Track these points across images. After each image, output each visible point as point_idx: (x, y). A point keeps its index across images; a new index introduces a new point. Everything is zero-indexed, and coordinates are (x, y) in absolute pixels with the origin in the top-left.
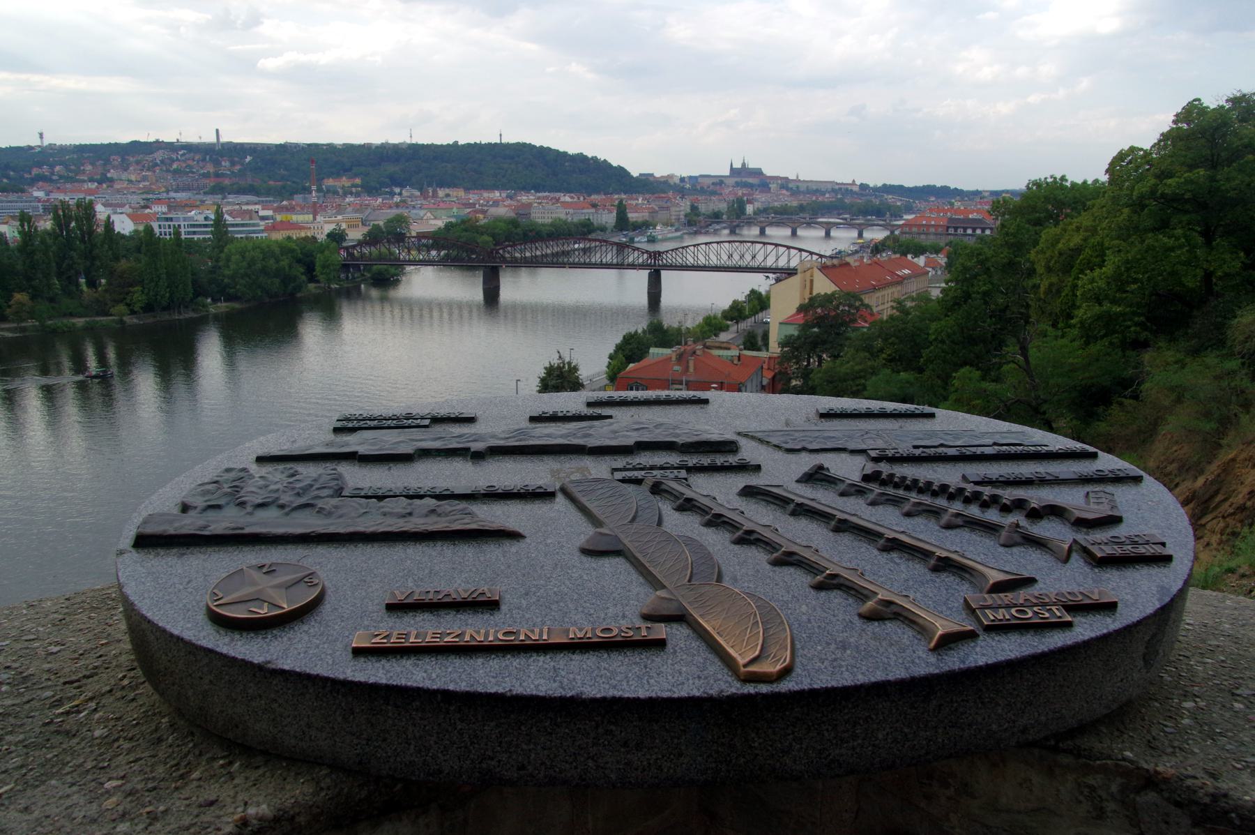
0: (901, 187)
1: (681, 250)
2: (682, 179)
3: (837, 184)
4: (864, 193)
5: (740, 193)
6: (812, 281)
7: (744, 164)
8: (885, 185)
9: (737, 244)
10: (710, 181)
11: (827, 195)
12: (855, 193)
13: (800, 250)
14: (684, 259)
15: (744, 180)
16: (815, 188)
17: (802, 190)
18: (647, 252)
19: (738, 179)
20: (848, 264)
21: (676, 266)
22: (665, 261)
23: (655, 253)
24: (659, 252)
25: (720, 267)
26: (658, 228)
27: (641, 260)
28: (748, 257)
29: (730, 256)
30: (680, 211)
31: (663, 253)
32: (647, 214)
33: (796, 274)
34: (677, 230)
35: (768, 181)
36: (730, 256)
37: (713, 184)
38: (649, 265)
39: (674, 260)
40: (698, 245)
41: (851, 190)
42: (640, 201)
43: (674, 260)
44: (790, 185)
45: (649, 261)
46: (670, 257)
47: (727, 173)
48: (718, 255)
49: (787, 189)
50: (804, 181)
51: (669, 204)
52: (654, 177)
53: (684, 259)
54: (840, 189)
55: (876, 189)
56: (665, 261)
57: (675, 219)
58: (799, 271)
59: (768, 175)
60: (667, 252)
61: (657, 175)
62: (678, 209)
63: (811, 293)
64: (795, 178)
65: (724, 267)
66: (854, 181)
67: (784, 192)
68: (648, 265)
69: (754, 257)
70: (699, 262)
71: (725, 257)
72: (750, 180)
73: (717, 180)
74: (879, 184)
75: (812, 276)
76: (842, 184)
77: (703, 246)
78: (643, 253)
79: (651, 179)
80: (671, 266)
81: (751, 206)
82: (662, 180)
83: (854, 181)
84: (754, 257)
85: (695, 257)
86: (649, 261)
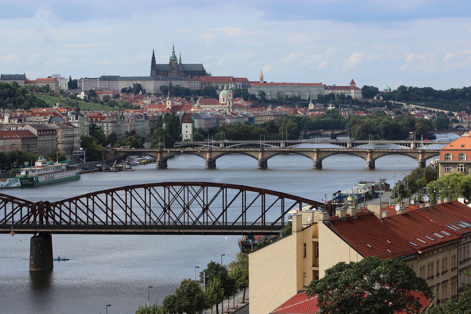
0: (428, 92)
1: (84, 200)
2: (73, 84)
3: (326, 88)
4: (370, 101)
5: (169, 104)
6: (316, 245)
7: (173, 59)
8: (402, 88)
9: (178, 188)
10: (122, 85)
11: (311, 106)
12: (356, 102)
13: (282, 196)
14: (91, 215)
15: (175, 83)
16: (290, 94)
17: (269, 98)
18: (27, 203)
19: (162, 83)
20: (371, 215)
21: (77, 226)
22: (57, 219)
23: (40, 204)
24: (47, 203)
25: (151, 227)
26: (38, 164)
27: (17, 218)
28: (196, 209)
29: (167, 208)
30: (73, 136)
31: (55, 205)
32: (19, 142)
33: (289, 233)
34: (69, 168)
35: (214, 85)
36: (167, 208)
37: (124, 90)
38: (34, 225)
39: (73, 217)
40: (114, 190)
41: (350, 97)
42: (6, 121)
43: (73, 217)
44: (252, 91)
45: (32, 219)
46: (67, 212)
47: (147, 73)
48: (147, 208)
49: (248, 97)
50: (272, 84)
51: (54, 125)
52: (27, 82)
53: (91, 215)
54: (332, 96)
55: (389, 95)
56: (57, 219)
57: (66, 149)
58: (294, 228)
59: (214, 74)
60: (62, 203)
61: (31, 77)
62: (69, 133)
63: (316, 264)
64: (258, 80)
65: (157, 227)
66: (353, 82)
67: (240, 102)
68: (28, 226)
69: (206, 209)
70: (115, 219)
71: (158, 211)
72: (185, 84)
73: (131, 85)
74: (394, 87)
75: (315, 236)
76: (334, 88)
77: (122, 193)
78: (21, 206)
79: (22, 84)
80: (69, 226)
81: (190, 125)
82: (41, 85)
83: (353, 82)
84: (206, 209)
85: (108, 209)
86: (32, 219)
